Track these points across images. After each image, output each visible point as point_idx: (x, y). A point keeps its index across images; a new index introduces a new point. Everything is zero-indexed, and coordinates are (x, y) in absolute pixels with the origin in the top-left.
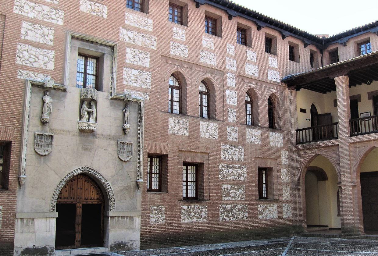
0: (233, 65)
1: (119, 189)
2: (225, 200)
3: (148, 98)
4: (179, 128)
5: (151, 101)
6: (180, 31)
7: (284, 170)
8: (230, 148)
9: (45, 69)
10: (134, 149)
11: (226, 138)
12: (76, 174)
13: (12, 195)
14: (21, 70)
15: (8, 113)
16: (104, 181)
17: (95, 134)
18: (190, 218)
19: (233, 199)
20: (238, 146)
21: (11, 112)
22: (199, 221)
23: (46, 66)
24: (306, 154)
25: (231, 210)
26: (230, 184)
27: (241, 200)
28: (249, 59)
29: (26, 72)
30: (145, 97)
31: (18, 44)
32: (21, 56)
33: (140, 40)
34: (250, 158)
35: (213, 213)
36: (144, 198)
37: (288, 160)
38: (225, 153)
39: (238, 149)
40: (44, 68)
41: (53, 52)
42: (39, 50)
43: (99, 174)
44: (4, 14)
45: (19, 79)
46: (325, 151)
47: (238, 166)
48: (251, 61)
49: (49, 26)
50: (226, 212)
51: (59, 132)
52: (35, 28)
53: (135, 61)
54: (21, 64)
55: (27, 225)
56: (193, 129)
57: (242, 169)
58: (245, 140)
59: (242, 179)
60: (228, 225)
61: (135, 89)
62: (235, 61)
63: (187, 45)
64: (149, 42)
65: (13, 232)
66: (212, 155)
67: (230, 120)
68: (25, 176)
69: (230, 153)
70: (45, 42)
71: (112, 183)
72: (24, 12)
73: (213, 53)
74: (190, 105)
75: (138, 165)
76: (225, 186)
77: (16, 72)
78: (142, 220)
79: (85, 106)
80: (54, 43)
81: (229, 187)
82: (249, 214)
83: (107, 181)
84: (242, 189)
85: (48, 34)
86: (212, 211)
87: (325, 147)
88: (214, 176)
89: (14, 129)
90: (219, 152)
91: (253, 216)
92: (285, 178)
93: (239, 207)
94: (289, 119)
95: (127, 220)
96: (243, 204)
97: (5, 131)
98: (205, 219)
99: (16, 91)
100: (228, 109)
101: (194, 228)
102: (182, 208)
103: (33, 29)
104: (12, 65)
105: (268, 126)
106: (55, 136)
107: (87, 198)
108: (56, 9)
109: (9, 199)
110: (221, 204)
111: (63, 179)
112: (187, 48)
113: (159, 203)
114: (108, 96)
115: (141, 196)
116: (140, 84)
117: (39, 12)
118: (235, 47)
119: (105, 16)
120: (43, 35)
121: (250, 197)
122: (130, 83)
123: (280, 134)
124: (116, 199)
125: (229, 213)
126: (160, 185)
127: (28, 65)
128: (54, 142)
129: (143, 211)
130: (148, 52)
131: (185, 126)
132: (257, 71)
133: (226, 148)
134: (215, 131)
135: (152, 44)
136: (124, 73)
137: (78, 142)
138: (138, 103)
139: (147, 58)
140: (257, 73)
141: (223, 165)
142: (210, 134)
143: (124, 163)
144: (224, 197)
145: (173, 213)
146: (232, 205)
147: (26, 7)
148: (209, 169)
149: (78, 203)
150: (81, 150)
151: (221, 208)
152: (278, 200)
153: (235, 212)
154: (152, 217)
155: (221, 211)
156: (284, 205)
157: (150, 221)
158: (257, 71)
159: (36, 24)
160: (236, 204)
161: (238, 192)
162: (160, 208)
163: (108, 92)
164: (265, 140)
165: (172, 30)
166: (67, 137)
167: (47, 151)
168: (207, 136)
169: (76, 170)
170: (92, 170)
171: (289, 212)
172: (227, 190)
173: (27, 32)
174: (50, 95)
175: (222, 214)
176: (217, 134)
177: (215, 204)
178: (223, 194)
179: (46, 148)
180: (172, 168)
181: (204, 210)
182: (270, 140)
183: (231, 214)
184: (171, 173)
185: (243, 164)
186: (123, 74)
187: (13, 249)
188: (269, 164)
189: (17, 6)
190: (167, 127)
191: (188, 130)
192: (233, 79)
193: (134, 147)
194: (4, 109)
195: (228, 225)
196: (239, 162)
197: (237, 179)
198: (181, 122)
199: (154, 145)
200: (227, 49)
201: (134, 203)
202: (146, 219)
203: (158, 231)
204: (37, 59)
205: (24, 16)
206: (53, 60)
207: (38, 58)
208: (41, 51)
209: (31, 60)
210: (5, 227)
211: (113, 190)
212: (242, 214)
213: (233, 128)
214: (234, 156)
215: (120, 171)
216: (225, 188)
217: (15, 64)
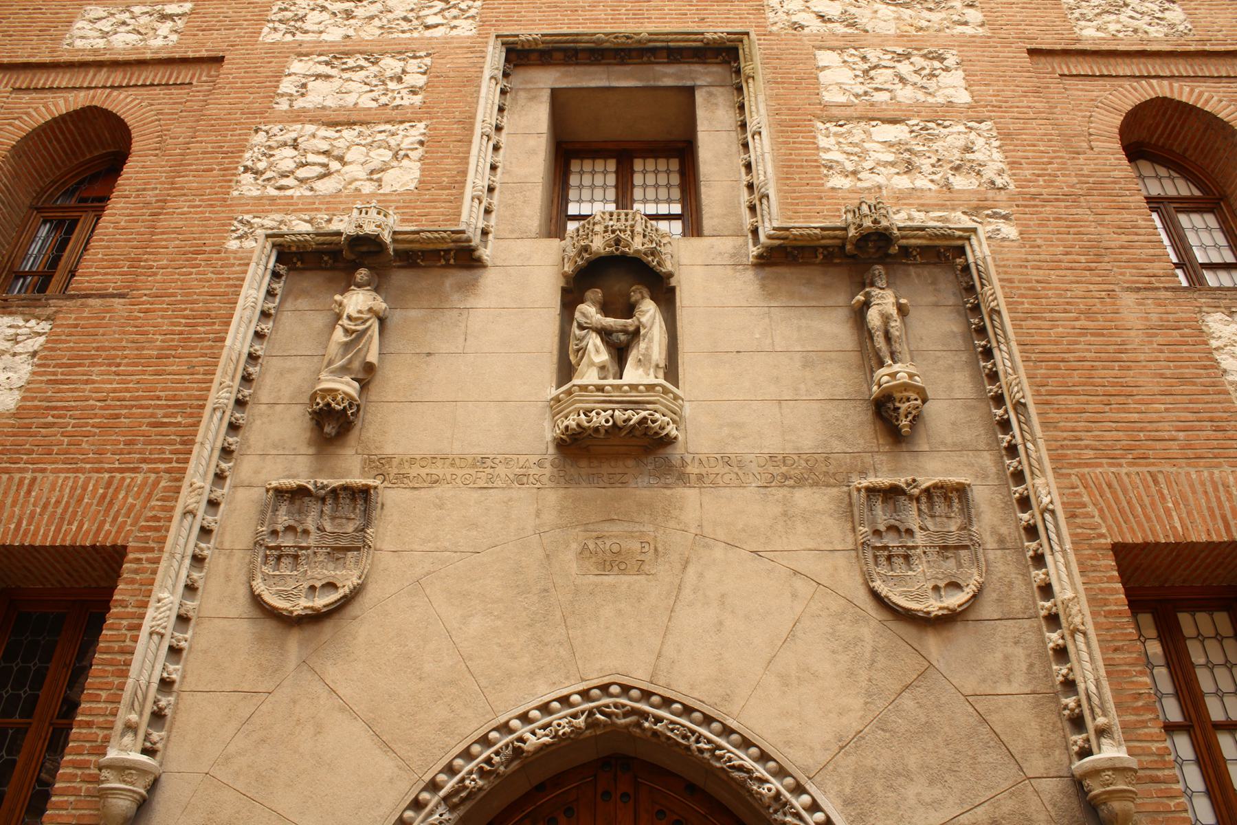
5: (1039, 242)
10: (994, 531)
12: (532, 742)
14: (247, 217)
15: (141, 407)
16: (775, 784)
17: (676, 460)
21: (159, 398)
23: (379, 180)
31: (257, 131)
42: (348, 134)
43: (732, 731)
51: (423, 472)
52: (344, 66)
53: (877, 89)
54: (256, 193)
72: (306, 32)
75: (1054, 637)
77: (224, 228)
79: (589, 311)
83: (799, 789)
89: (156, 483)
97: (104, 496)
104: (211, 206)
111: (433, 786)
120: (374, 83)
127: (289, 192)
128: (384, 532)
135: (956, 18)
136: (823, 142)
137: (549, 517)
139: (947, 69)
143: (932, 643)
150: (574, 567)
159: (348, 54)
163: (738, 234)
166: (476, 495)
167: (332, 586)
169: (535, 714)
170: (667, 702)
173: (304, 86)
179: (323, 572)
186: (818, 148)
190: (1205, 367)
194: (127, 390)
199: (1147, 487)
204: (335, 165)
207: (341, 159)
208: (360, 134)
215: (907, 702)
217: (225, 200)
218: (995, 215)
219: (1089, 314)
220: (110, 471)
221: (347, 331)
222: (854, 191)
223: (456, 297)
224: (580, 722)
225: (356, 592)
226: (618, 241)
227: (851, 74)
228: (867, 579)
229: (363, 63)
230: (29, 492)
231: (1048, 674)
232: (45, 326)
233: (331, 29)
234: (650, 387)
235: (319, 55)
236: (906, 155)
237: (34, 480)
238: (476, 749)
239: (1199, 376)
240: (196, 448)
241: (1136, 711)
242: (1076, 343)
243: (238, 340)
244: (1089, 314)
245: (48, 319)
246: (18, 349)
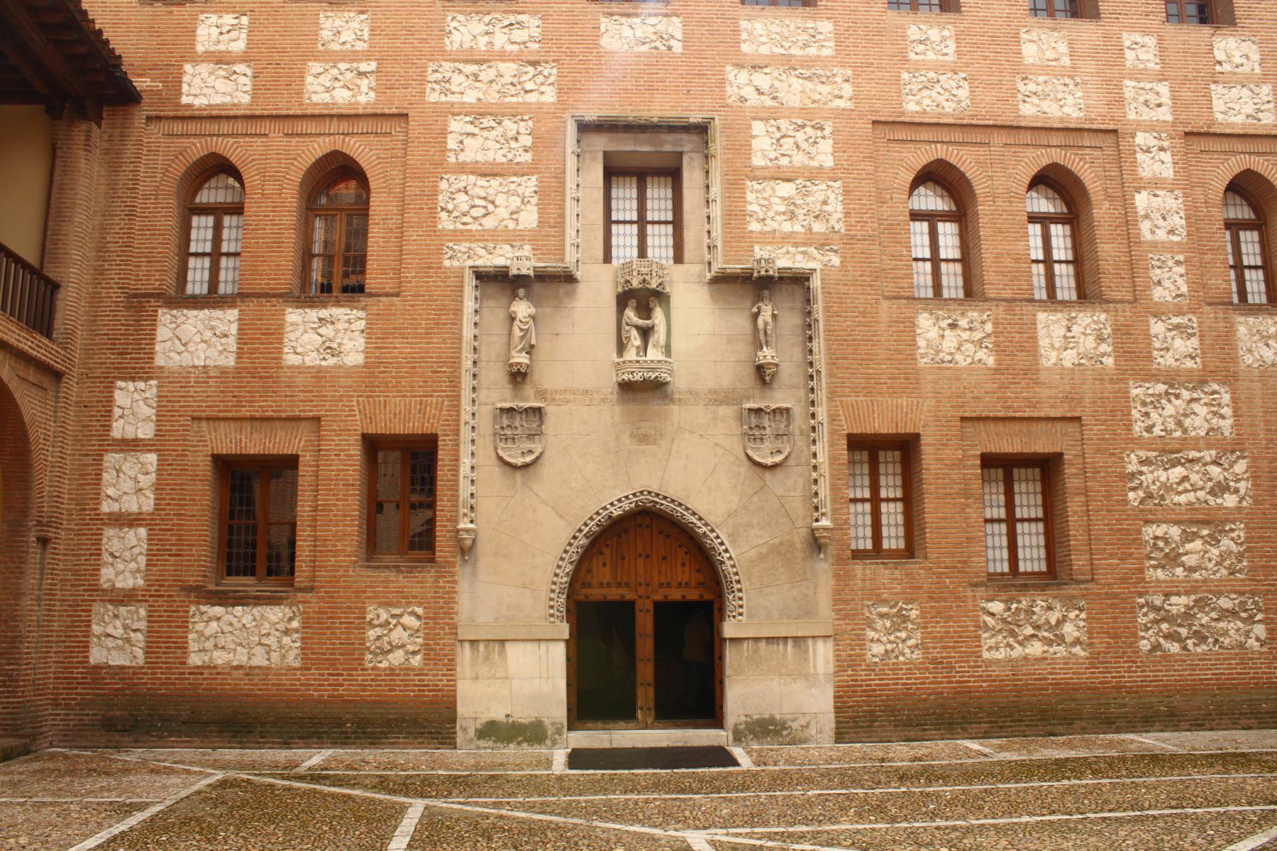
0: (1158, 102)
1: (753, 553)
2: (1158, 581)
3: (836, 261)
4: (955, 344)
5: (850, 268)
6: (934, 34)
8: (1171, 394)
9: (515, 230)
10: (800, 427)
11: (1150, 358)
12: (616, 513)
13: (445, 577)
14: (451, 244)
16: (704, 529)
17: (670, 392)
18: (1020, 643)
19: (1196, 576)
20: (1203, 382)
22: (1055, 653)
23: (516, 220)
25: (1188, 615)
26: (1177, 523)
27: (1228, 580)
28: (1227, 67)
29: (463, 247)
30: (826, 259)
31: (442, 178)
32: (450, 207)
33: (794, 91)
34: (1262, 424)
35: (1112, 628)
36: (842, 579)
38: (1147, 414)
39: (1206, 393)
40: (511, 225)
41: (534, 178)
42: (495, 182)
44: (405, 112)
45: (449, 268)
47: (1208, 455)
48: (1235, 73)
49: (515, 113)
50: (1168, 622)
52: (482, 126)
53: (783, 155)
54: (452, 227)
55: (487, 658)
56: (1010, 342)
57: (1227, 466)
58: (1235, 359)
59: (1230, 501)
60: (1175, 671)
61: (788, 238)
62: (1164, 89)
63: (962, 71)
64: (825, 89)
65: (452, 675)
66: (1096, 425)
67: (1158, 294)
68: (472, 526)
70: (510, 156)
71: (729, 536)
72: (453, 93)
73: (1069, 76)
74: (995, 262)
77: (439, 251)
78: (838, 650)
79: (630, 314)
80: (533, 156)
81: (1175, 532)
82: (1269, 631)
83: (712, 531)
84: (1232, 539)
85: (518, 133)
86: (1107, 618)
88: (1109, 497)
90: (1122, 411)
93: (1225, 603)
95: (786, 649)
96: (1242, 593)
97: (420, 410)
98: (1078, 648)
99: (442, 300)
100: (1151, 256)
101: (1035, 679)
102: (983, 609)
103: (476, 131)
104: (429, 235)
106: (550, 410)
107: (668, 584)
108: (534, 64)
109: (438, 587)
110: (1141, 595)
111: (580, 531)
112: (965, 79)
113: (897, 593)
114: (701, 275)
115: (830, 575)
116: (804, 223)
117: (491, 82)
118: (1160, 40)
119: (678, 47)
120: (502, 141)
122: (771, 225)
124: (744, 585)
125: (1180, 625)
126: (909, 537)
127: (469, 227)
128: (550, 426)
129: (842, 622)
130: (827, 119)
131: (978, 335)
132: (1268, 102)
133: (1152, 395)
134: (1101, 339)
135: (836, 92)
136: (750, 197)
137: (617, 419)
138: (798, 281)
139: (824, 138)
140: (1268, 110)
141: (1143, 454)
143: (768, 475)
144: (1155, 567)
145: (953, 627)
146: (1193, 597)
147: (457, 79)
148: (1086, 472)
149: (641, 597)
150: (628, 442)
151: (1142, 607)
153: (1205, 620)
154: (872, 640)
155: (1142, 620)
157: (864, 655)
158: (1268, 102)
159: (483, 115)
161: (1215, 552)
162: (902, 609)
163: (701, 262)
165: (904, 37)
166: (585, 408)
167: (530, 452)
168: (1069, 358)
170: (665, 498)
172: (1167, 542)
173: (461, 142)
174: (528, 297)
175: (1147, 629)
176: (1109, 349)
177: (1115, 596)
178: (1151, 558)
179: (528, 445)
180: (938, 479)
181: (1072, 615)
183: (1190, 629)
184: (937, 493)
185: (1228, 449)
186: (746, 202)
187: (455, 723)
189: (435, 82)
190: (910, 345)
191: (990, 346)
192: (1162, 149)
193: (799, 420)
194: (416, 353)
195: (1175, 671)
196: (1211, 438)
197: (1206, 502)
198: (963, 323)
199: (868, 407)
200: (1127, 51)
201: (806, 596)
202: (850, 645)
203: (897, 684)
204: (491, 207)
205: (452, 104)
206: (534, 200)
207: (493, 202)
208: (501, 184)
209: (475, 212)
210: (432, 662)
211: (733, 556)
212: (1238, 630)
213: (1175, 320)
214: (1187, 422)
215: (755, 499)
216: (1156, 538)
217: (435, 231)
218: (831, 250)
219: (863, 314)
220: (420, 396)
221: (521, 330)
222: (761, 233)
223: (566, 300)
224: (633, 505)
225: (541, 454)
226: (644, 281)
227: (769, 141)
228: (745, 448)
229: (493, 124)
230: (385, 407)
231: (810, 489)
232: (362, 314)
233: (468, 91)
234: (659, 362)
235: (466, 115)
236: (792, 207)
237: (385, 401)
238: (595, 516)
239: (906, 350)
240: (463, 392)
241: (841, 503)
242: (855, 330)
243: (468, 331)
244: (863, 314)
245: (362, 309)
246: (353, 327)
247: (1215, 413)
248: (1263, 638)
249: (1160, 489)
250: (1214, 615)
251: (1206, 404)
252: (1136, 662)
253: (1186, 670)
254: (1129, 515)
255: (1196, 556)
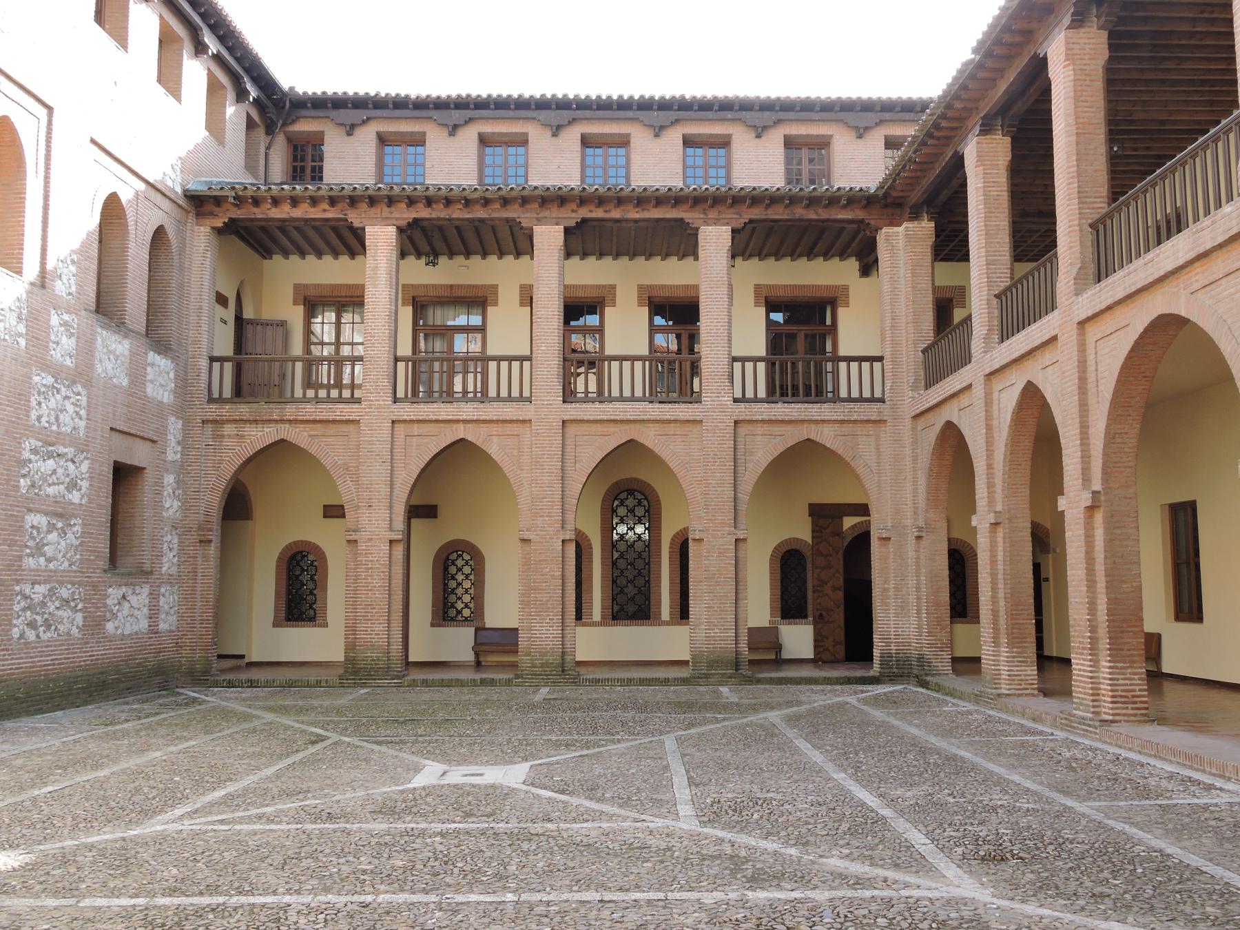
7: (169, 479)
19: (51, 566)
20: (74, 382)
24: (243, 436)
25: (43, 604)
26: (46, 514)
27: (68, 572)
37: (179, 448)
38: (39, 404)
46: (310, 436)
47: (70, 451)
58: (91, 366)
59: (75, 497)
60: (31, 658)
69: (52, 404)
76: (33, 519)
82: (85, 618)
87: (315, 421)
91: (94, 624)
92: (171, 506)
93: (64, 593)
94: (193, 319)
96: (73, 584)
105: (143, 330)
110: (18, 582)
121: (90, 560)
123: (169, 362)
125: (38, 614)
133: (45, 385)
134: (20, 318)
142: (7, 326)
144: (28, 555)
146: (48, 586)
151: (17, 595)
152: (151, 573)
155: (17, 608)
156: (163, 590)
160: (57, 582)
161: (63, 543)
164: (137, 375)
171: (172, 611)
175: (19, 616)
178: (26, 546)
182: (149, 378)
188: (138, 455)
196: (71, 440)
197: (64, 497)
214: (61, 417)
216: (33, 527)
247: (77, 413)
248: (80, 625)
249: (40, 479)
250: (57, 604)
251: (73, 403)
252: (8, 650)
253: (36, 657)
254: (19, 502)
255: (53, 547)
